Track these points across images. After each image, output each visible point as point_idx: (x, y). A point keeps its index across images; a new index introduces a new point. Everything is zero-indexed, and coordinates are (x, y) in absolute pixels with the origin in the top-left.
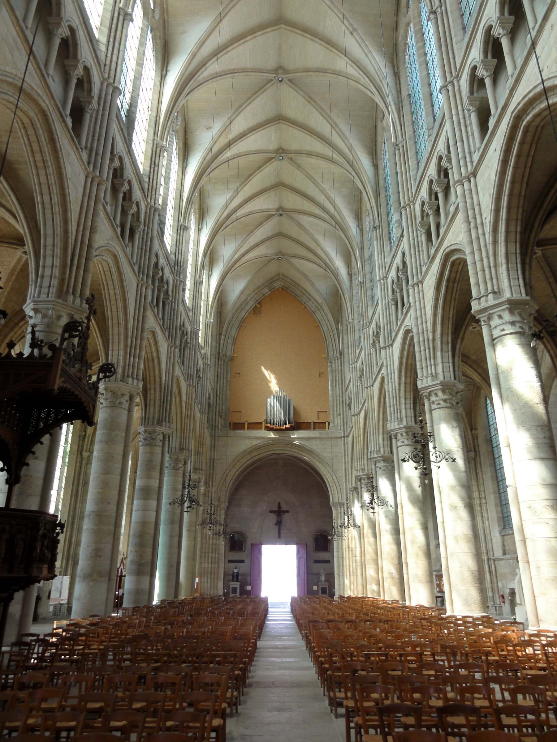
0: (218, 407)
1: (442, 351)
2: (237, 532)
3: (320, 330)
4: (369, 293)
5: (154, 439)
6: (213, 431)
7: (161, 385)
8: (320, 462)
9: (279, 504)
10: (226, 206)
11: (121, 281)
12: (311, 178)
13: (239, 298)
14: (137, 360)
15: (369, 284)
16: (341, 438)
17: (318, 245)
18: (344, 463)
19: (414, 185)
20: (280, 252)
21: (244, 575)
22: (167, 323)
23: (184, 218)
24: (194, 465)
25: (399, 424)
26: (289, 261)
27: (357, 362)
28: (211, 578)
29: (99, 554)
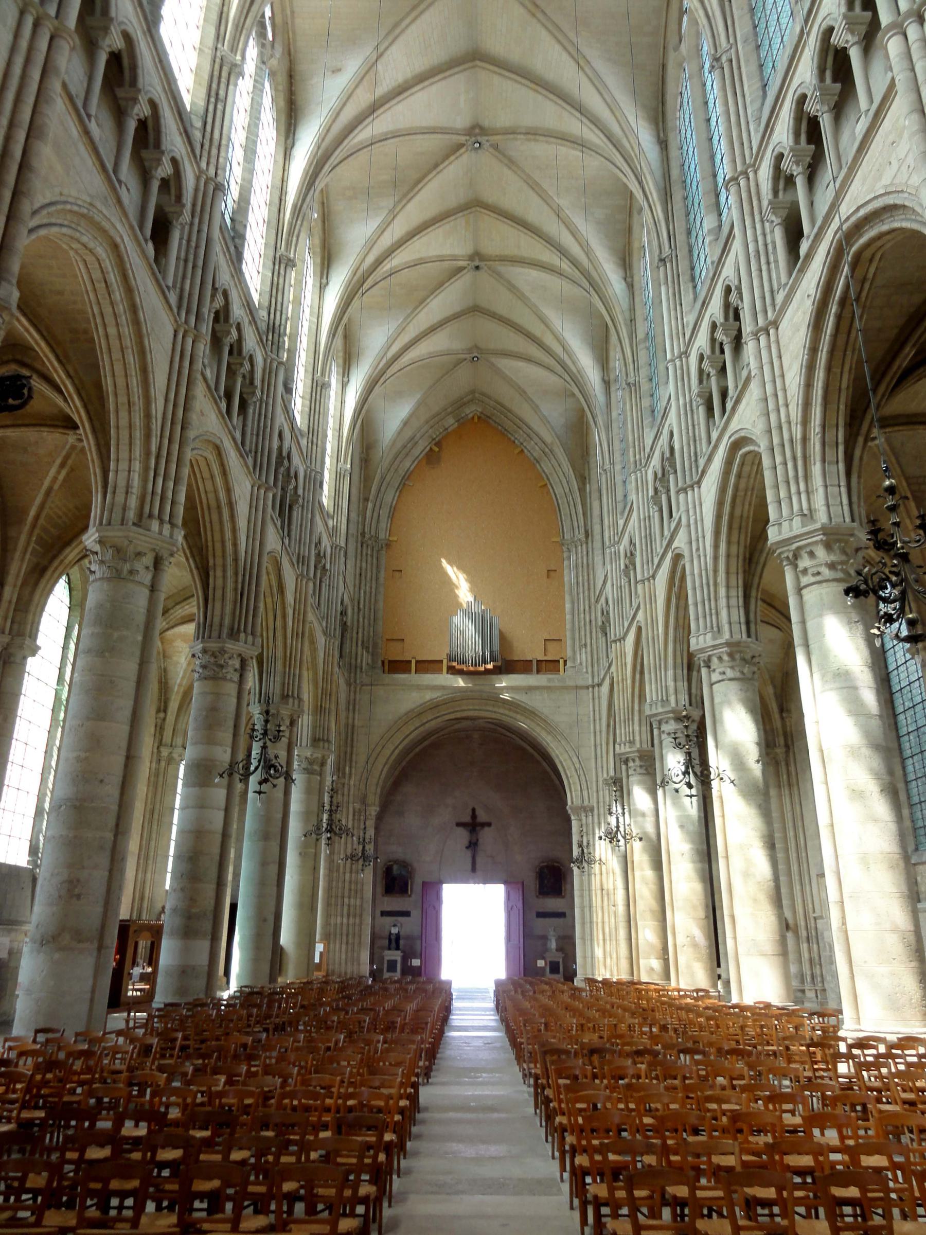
0: (360, 631)
1: (823, 460)
2: (396, 862)
3: (548, 492)
4: (646, 402)
5: (222, 667)
6: (352, 675)
7: (236, 560)
8: (549, 733)
9: (474, 810)
10: (371, 244)
11: (134, 309)
12: (534, 186)
13: (400, 432)
14: (171, 484)
15: (645, 386)
16: (588, 688)
17: (547, 326)
19: (757, 131)
20: (477, 347)
21: (409, 938)
22: (251, 443)
23: (288, 244)
24: (314, 733)
25: (714, 638)
26: (493, 364)
27: (619, 542)
28: (347, 943)
29: (77, 891)
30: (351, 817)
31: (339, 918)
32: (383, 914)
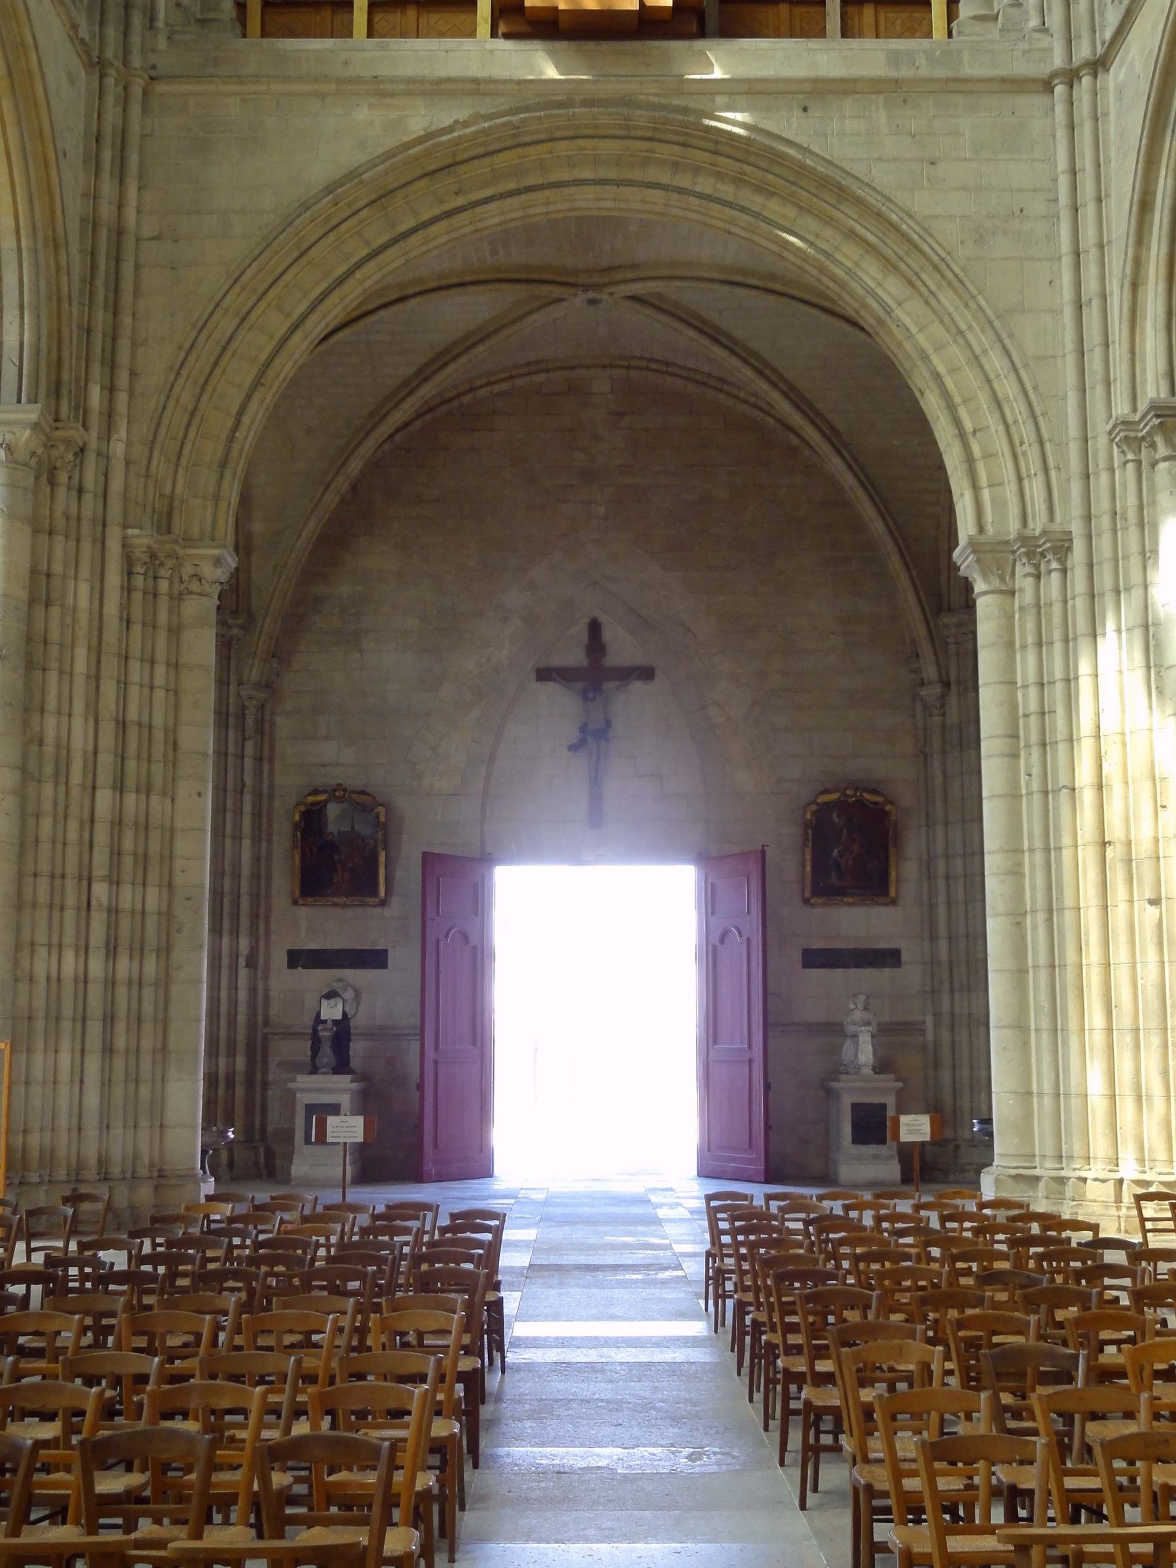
2: (337, 792)
8: (890, 266)
9: (595, 628)
18: (1067, 262)
21: (379, 1034)
28: (108, 1050)
30: (114, 579)
31: (69, 956)
32: (297, 959)
